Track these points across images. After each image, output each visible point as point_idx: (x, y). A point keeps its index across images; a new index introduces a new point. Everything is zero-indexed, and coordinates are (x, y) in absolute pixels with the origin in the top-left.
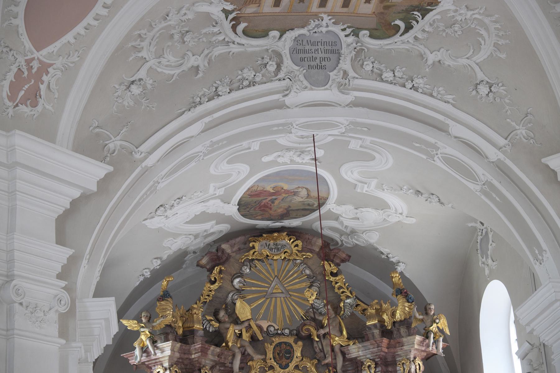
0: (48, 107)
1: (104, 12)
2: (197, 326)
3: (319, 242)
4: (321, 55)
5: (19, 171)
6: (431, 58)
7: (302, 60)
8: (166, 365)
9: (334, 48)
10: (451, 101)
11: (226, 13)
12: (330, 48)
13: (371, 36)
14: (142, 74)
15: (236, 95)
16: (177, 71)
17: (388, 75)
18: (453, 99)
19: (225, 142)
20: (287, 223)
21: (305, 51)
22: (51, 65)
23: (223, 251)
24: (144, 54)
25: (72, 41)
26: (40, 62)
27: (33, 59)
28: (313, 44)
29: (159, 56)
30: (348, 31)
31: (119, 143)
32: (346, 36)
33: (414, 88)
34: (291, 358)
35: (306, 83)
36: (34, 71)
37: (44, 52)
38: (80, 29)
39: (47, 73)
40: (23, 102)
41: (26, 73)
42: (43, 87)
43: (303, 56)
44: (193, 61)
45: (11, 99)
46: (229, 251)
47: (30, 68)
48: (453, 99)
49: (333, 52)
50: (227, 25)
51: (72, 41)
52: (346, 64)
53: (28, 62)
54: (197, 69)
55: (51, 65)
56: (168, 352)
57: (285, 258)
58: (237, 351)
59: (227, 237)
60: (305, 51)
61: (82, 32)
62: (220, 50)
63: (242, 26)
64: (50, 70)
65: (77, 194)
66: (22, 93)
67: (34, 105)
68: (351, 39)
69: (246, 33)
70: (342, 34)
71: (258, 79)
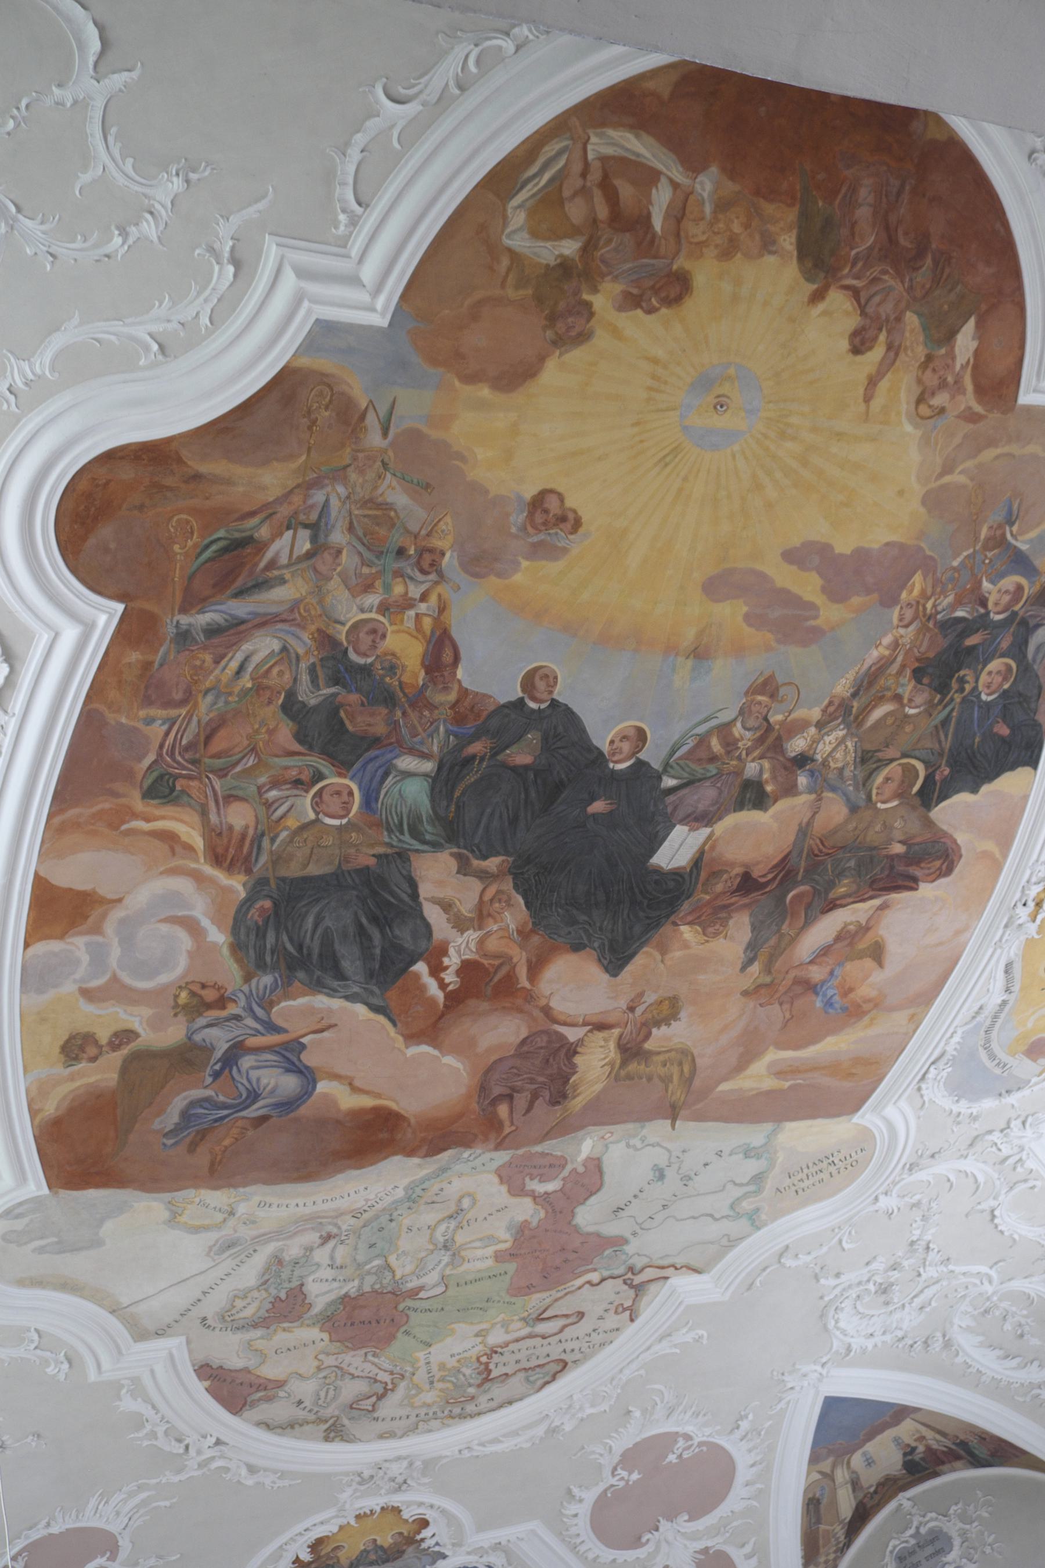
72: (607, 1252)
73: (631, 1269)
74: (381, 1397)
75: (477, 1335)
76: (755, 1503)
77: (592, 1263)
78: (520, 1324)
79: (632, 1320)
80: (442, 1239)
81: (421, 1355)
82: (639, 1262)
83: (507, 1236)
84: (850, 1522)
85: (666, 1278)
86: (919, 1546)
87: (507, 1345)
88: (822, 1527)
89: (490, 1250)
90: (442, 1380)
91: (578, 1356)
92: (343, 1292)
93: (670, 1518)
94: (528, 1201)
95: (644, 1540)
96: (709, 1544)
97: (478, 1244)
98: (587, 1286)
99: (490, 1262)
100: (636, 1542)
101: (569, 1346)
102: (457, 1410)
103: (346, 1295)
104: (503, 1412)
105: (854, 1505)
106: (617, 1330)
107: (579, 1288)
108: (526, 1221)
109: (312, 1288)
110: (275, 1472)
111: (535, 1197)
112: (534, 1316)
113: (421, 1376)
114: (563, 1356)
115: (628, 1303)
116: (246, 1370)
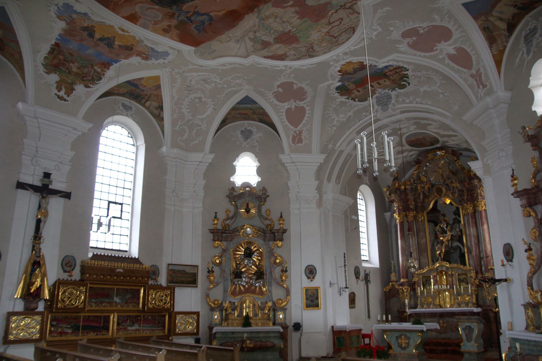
0: (307, 142)
1: (310, 112)
2: (407, 187)
3: (450, 150)
4: (385, 100)
5: (296, 163)
6: (422, 90)
7: (380, 104)
8: (397, 201)
9: (390, 97)
10: (430, 104)
11: (348, 98)
12: (387, 97)
13: (399, 89)
14: (335, 123)
15: (361, 122)
16: (345, 119)
17: (407, 101)
18: (431, 103)
19: (369, 135)
20: (435, 146)
21: (380, 101)
22: (302, 130)
23: (419, 160)
24: (333, 117)
25: (306, 122)
26: (299, 131)
27: (296, 131)
28: (382, 97)
29: (338, 116)
30: (391, 90)
31: (331, 146)
32: (392, 91)
33: (417, 103)
34: (442, 192)
35: (381, 111)
36: (298, 133)
37: (298, 128)
38: (306, 118)
39: (302, 133)
40: (298, 143)
41: (296, 135)
42: (303, 137)
43: (380, 102)
44: (349, 114)
45: (293, 143)
46: (422, 159)
47: (296, 134)
48: (431, 103)
49: (389, 98)
50: (352, 102)
51: (306, 122)
52: (393, 101)
53: (295, 132)
54: (350, 117)
55: (302, 130)
56: (394, 198)
57: (439, 158)
58: (421, 193)
59: (418, 155)
60: (380, 101)
61: (307, 119)
62: (356, 109)
63: (356, 100)
64: (303, 132)
65: (319, 164)
66: (296, 141)
67: (301, 142)
68: (394, 92)
69: (359, 101)
70: (390, 92)
71: (368, 114)
72: (328, 6)
73: (341, 6)
74: (312, 48)
75: (318, 31)
76: (463, 34)
77: (327, 10)
78: (327, 26)
79: (359, 14)
80: (281, 22)
81: (310, 39)
82: (343, 4)
83: (295, 15)
84: (507, 29)
85: (356, 3)
86: (530, 33)
87: (330, 30)
88: (494, 34)
89: (295, 19)
90: (322, 41)
91: (354, 25)
92: (273, 37)
93: (439, 42)
94: (289, 8)
95: (434, 49)
96: (456, 46)
97: (290, 19)
98: (333, 14)
99: (299, 21)
100: (432, 50)
101: (349, 24)
102: (336, 44)
103: (275, 38)
104: (350, 40)
105: (506, 24)
106: (358, 17)
107: (332, 15)
108: (295, 11)
109: (267, 39)
110: (309, 65)
111: (291, 6)
112: (328, 24)
113: (315, 42)
114: (349, 27)
115: (352, 12)
116: (273, 55)
